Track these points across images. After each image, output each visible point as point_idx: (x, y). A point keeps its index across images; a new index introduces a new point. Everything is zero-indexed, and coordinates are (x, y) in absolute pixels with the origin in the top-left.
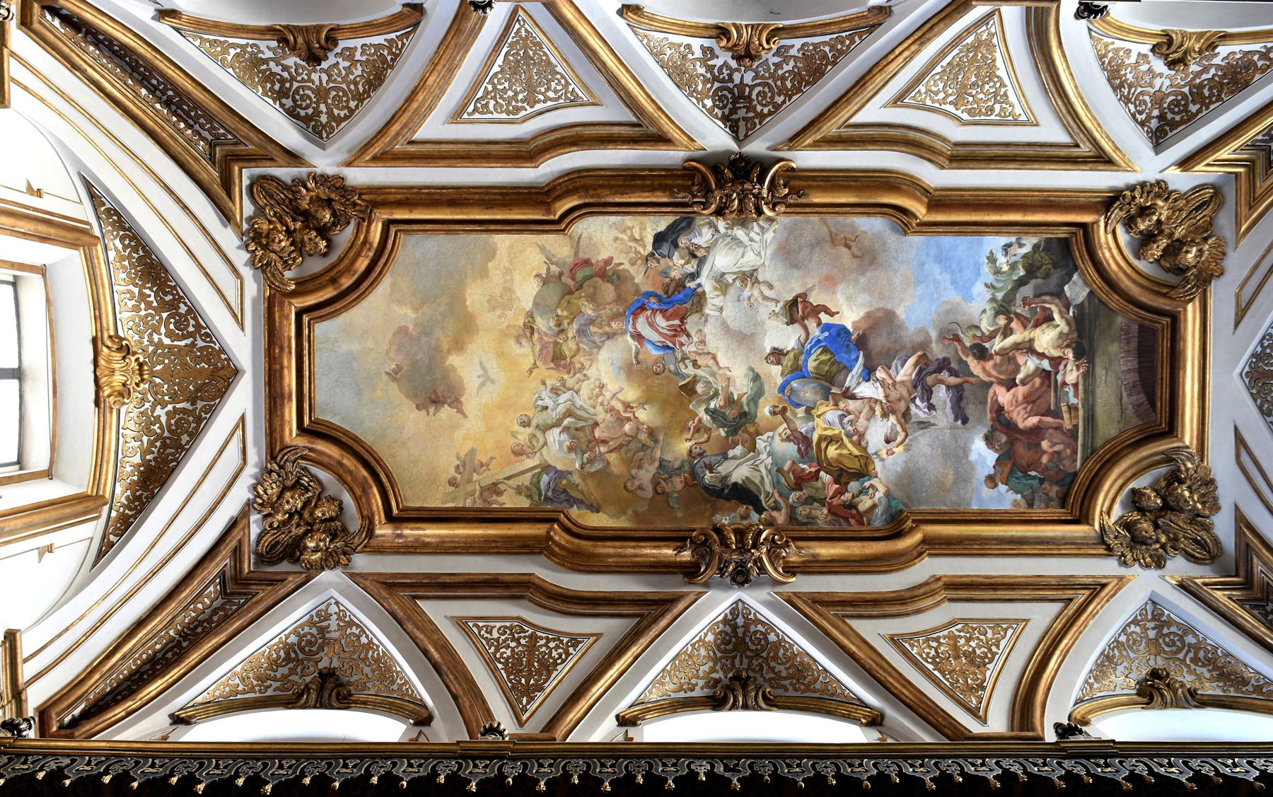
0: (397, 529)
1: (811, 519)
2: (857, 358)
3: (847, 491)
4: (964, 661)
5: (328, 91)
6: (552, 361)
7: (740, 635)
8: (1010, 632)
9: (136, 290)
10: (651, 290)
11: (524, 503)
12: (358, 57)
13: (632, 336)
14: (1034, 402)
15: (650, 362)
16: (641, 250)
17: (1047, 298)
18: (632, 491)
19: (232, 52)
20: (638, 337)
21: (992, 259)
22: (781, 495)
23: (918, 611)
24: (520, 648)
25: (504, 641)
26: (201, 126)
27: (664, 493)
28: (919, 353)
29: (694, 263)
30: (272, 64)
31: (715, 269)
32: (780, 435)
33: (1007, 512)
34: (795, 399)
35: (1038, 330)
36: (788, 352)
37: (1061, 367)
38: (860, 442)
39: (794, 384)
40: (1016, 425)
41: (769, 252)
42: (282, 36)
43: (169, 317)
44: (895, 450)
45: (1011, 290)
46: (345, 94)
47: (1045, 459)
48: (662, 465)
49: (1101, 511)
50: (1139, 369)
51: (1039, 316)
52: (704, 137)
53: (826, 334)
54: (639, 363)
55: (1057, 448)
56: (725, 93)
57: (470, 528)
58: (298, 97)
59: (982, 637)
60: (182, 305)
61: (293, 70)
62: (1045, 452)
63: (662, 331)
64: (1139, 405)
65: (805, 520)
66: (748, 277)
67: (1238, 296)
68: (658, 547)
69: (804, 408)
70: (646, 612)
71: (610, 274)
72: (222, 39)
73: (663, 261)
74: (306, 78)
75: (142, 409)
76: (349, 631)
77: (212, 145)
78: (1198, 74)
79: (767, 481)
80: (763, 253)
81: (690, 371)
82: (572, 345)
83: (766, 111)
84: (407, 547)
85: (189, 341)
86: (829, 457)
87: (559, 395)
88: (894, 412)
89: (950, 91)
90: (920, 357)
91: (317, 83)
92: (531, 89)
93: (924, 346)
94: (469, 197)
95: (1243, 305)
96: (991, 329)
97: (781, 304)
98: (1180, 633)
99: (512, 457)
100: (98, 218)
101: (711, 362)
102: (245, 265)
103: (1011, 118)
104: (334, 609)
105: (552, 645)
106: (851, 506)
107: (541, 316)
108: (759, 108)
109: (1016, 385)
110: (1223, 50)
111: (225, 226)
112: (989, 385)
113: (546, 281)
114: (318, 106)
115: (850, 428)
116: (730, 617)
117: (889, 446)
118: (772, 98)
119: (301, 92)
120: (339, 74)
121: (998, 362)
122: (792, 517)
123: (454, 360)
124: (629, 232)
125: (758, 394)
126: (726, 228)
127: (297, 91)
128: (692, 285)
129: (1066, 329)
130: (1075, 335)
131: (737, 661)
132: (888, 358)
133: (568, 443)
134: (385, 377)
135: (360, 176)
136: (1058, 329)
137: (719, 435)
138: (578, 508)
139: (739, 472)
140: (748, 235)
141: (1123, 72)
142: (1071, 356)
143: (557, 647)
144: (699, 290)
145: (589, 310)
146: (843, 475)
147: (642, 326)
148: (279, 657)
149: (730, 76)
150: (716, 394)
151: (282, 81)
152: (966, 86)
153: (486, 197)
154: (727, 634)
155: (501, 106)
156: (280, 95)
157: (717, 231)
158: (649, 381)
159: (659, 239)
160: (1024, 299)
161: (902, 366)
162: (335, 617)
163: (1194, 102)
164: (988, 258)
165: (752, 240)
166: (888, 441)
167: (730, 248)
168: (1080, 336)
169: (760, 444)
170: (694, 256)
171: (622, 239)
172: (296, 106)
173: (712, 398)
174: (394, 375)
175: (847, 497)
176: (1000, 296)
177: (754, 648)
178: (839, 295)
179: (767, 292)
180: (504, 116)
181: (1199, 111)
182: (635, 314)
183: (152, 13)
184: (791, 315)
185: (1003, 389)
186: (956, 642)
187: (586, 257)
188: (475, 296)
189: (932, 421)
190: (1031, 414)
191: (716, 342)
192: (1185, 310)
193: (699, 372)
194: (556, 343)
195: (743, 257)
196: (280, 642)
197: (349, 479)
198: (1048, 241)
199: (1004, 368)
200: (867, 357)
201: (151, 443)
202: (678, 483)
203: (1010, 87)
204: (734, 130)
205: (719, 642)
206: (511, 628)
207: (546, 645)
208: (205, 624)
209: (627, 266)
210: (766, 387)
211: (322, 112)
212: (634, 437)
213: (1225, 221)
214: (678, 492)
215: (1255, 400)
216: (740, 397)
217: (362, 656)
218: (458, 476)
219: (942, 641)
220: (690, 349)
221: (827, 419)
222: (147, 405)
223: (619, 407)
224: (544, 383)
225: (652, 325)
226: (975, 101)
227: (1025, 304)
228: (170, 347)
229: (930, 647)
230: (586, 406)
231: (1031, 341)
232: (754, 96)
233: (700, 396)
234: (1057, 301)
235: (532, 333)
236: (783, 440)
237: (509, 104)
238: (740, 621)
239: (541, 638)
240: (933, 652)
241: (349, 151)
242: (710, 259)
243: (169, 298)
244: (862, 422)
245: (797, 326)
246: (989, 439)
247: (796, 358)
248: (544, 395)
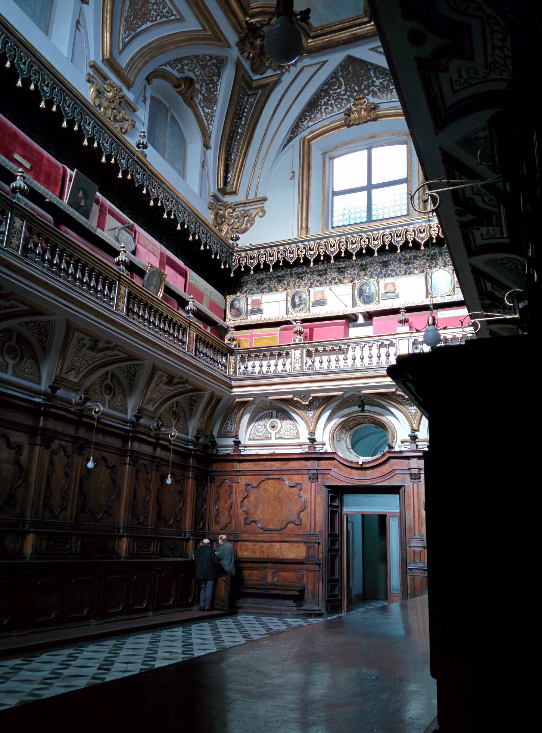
9: (323, 108)
12: (180, 66)
19: (207, 111)
26: (243, 102)
30: (203, 92)
42: (190, 101)
43: (332, 90)
58: (211, 75)
61: (201, 83)
72: (204, 118)
74: (201, 77)
75: (377, 91)
77: (249, 95)
85: (341, 79)
91: (200, 71)
100: (297, 135)
102: (296, 67)
111: (282, 81)
114: (210, 65)
127: (208, 77)
135: (232, 37)
151: (207, 84)
155: (163, 6)
156: (215, 84)
183: (209, 151)
211: (212, 63)
222: (375, 89)
228: (346, 85)
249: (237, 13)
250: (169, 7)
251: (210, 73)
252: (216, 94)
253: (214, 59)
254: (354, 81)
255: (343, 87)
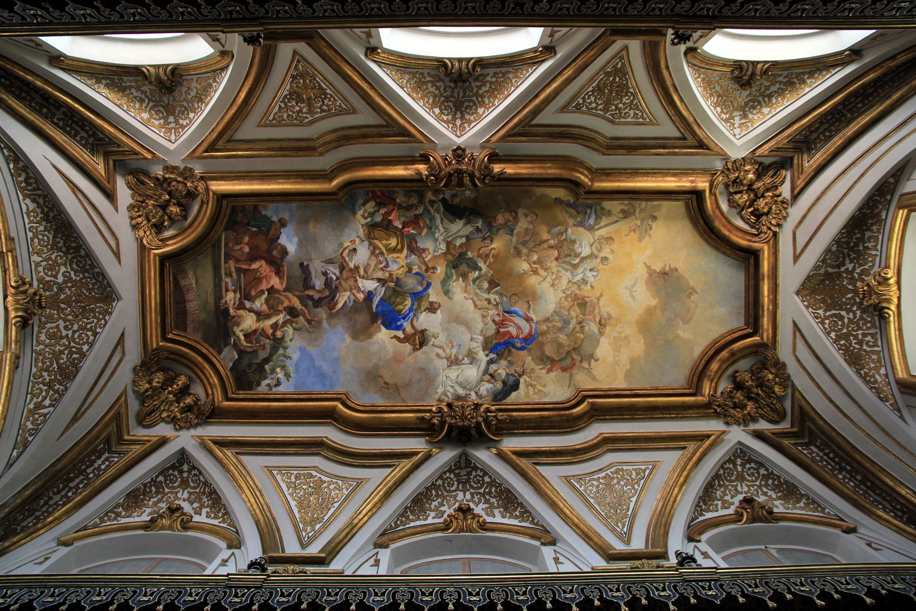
0: (694, 187)
1: (408, 194)
2: (377, 307)
3: (383, 215)
4: (304, 96)
5: (737, 479)
6: (586, 302)
7: (458, 113)
8: (271, 118)
10: (520, 352)
11: (607, 205)
12: (720, 503)
13: (532, 320)
14: (255, 279)
15: (520, 303)
16: (528, 379)
17: (249, 350)
18: (532, 213)
20: (528, 320)
21: (287, 376)
22: (429, 211)
23: (334, 131)
24: (616, 103)
25: (625, 109)
27: (510, 212)
28: (334, 311)
29: (491, 371)
30: (774, 496)
31: (477, 367)
32: (429, 253)
33: (272, 202)
34: (420, 278)
35: (254, 328)
36: (425, 311)
37: (237, 303)
38: (374, 249)
39: (420, 289)
40: (267, 262)
41: (440, 379)
44: (350, 244)
45: (273, 355)
46: (725, 478)
47: (246, 239)
48: (511, 232)
49: (208, 204)
50: (185, 303)
51: (253, 338)
52: (490, 456)
53: (399, 323)
54: (528, 302)
55: (238, 247)
56: (475, 486)
57: (645, 187)
58: (756, 475)
59: (291, 113)
60: (834, 337)
61: (760, 493)
62: (247, 244)
63: (512, 324)
64: (184, 278)
65: (413, 194)
66: (454, 362)
67: (124, 354)
68: (517, 174)
69: (413, 272)
70: (527, 128)
71: (548, 362)
73: (513, 372)
75: (862, 268)
76: (728, 116)
78: (160, 501)
79: (439, 221)
80: (444, 378)
81: (492, 297)
82: (573, 314)
83: (448, 474)
84: (687, 174)
86: (395, 239)
87: (582, 279)
88: (351, 270)
89: (326, 490)
90: (334, 308)
91: (744, 485)
92: (609, 486)
93: (331, 316)
94: (644, 413)
95: (119, 347)
96: (286, 328)
97: (431, 343)
98: (152, 120)
99: (614, 237)
101: (478, 303)
103: (283, 472)
104: (737, 131)
105: (594, 105)
106: (380, 205)
107: (594, 333)
108: (452, 476)
109: (268, 290)
110: (146, 518)
112: (285, 290)
113: (591, 356)
114: (742, 469)
115: (381, 258)
116: (466, 125)
117: (354, 246)
118: (444, 483)
119: (754, 478)
120: (730, 490)
121: (280, 306)
122: (421, 196)
123: (654, 302)
124: (536, 391)
125: (445, 282)
126: (470, 395)
127: (757, 479)
128: (492, 356)
129: (235, 329)
130: (229, 325)
131: (461, 95)
132: (355, 308)
133: (576, 246)
134: (698, 291)
136: (240, 328)
137: (472, 253)
138: (570, 201)
139: (458, 227)
140: (455, 390)
141: (210, 502)
142: (231, 311)
143: (590, 103)
144: (487, 352)
145: (562, 337)
146: (386, 226)
147: (526, 327)
148: (776, 98)
149: (473, 497)
150: (474, 281)
151: (767, 485)
152: (316, 494)
153: (633, 412)
154: (468, 113)
155: (627, 474)
157: (476, 393)
158: (520, 289)
159: (515, 386)
160: (264, 349)
161: (346, 302)
162: (736, 126)
163: (161, 482)
164: (290, 376)
165: (452, 387)
166: (355, 250)
167: (467, 381)
168: (226, 324)
169: (443, 247)
170: (491, 375)
171: (541, 386)
172: (757, 470)
173: (477, 278)
174: (693, 291)
175: (383, 211)
176: (281, 351)
177: (449, 104)
178: (391, 350)
179: (440, 351)
180: (625, 468)
181: (157, 477)
182: (530, 334)
184: (424, 336)
185: (276, 287)
186: (309, 110)
187: (564, 374)
188: (638, 346)
189: (324, 264)
190: (257, 270)
191: (475, 317)
192: (157, 344)
193: (486, 296)
194: (584, 314)
195: (458, 376)
196: (775, 108)
197: (724, 220)
198: (251, 389)
199: (276, 302)
200: (370, 307)
201: (857, 245)
202: (500, 219)
203: (286, 493)
204: (468, 463)
205: (474, 108)
206: (621, 117)
207: (598, 105)
208: (825, 121)
209: (537, 368)
210: (439, 286)
212: (531, 251)
213: (134, 405)
214: (500, 212)
215: (108, 283)
216: (457, 279)
217: (720, 99)
218: (650, 223)
219: (319, 110)
220: (492, 312)
221: (398, 264)
222: (858, 270)
223: (541, 272)
224: (592, 287)
225: (519, 328)
226: (309, 483)
227: (264, 345)
228: (841, 309)
229: (328, 105)
230: (564, 271)
231: (258, 320)
232: (456, 483)
233: (486, 280)
234: (242, 348)
235: (600, 321)
236: (428, 249)
237: (623, 476)
238: (458, 122)
239: (600, 110)
240: (326, 102)
241: (722, 441)
242: (480, 374)
243: (842, 342)
244: (373, 263)
245: (420, 329)
246: (285, 252)
247: (419, 306)
248: (592, 279)
249: (683, 402)
250: (633, 469)
251: (753, 474)
252: (784, 479)
253: (735, 459)
254: (837, 297)
255: (843, 313)
